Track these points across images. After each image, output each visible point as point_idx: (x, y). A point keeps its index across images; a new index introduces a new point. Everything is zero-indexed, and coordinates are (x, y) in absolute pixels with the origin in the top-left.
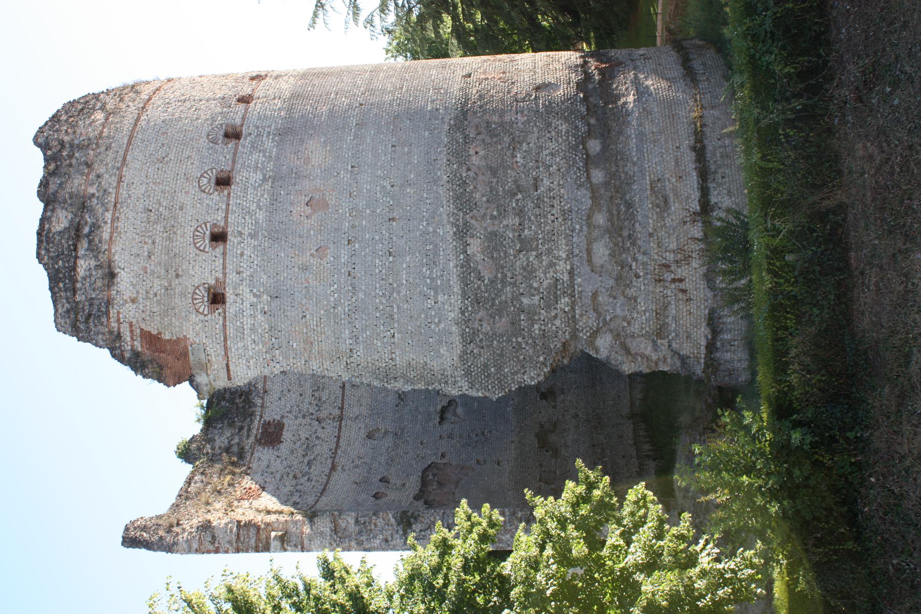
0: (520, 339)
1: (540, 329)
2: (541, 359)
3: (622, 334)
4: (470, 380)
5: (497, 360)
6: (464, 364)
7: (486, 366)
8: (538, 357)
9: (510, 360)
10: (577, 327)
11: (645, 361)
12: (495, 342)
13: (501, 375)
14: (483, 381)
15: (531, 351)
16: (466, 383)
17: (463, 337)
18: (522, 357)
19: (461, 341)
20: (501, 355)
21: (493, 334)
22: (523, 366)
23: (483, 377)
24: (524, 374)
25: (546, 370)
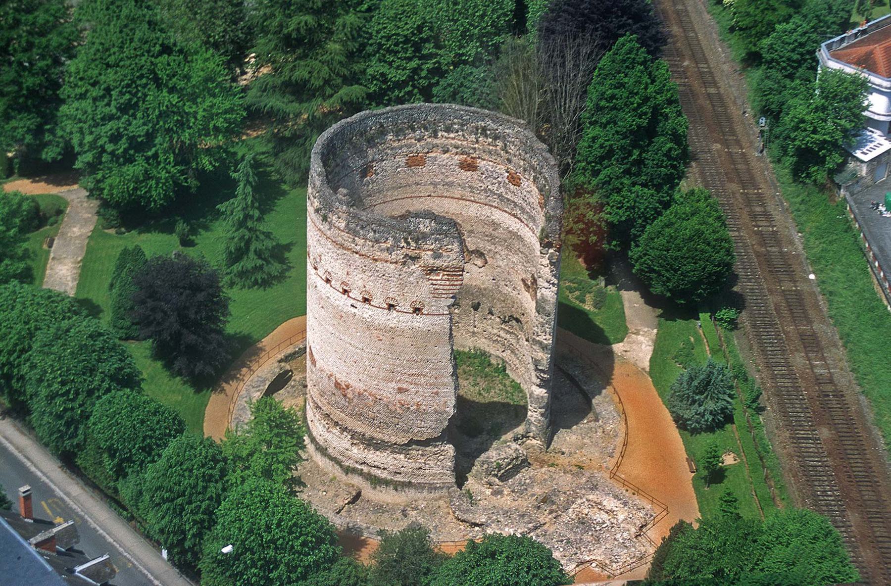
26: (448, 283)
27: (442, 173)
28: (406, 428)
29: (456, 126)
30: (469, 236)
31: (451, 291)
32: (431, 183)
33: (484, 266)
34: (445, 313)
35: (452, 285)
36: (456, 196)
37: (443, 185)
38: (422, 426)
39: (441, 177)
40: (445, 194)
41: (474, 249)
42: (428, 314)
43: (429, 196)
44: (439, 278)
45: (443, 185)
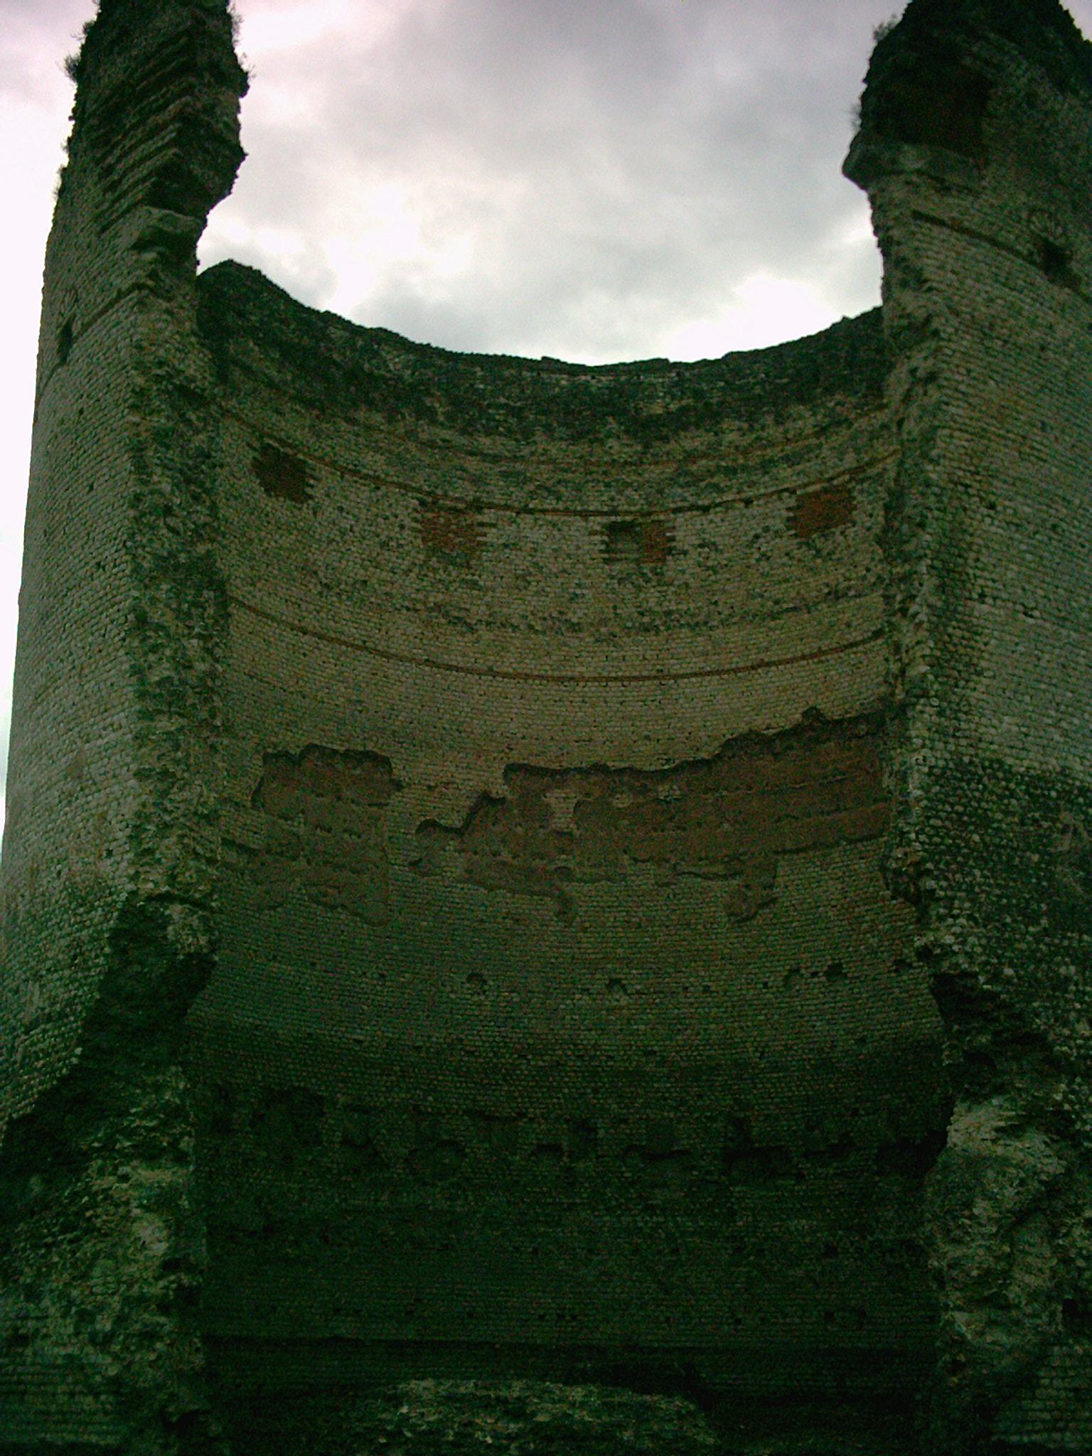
0: (1044, 922)
1: (1068, 979)
2: (1009, 971)
3: (1059, 1205)
4: (949, 773)
5: (999, 855)
6: (984, 768)
7: (984, 822)
8: (1011, 965)
9: (998, 885)
10: (1078, 1080)
11: (1002, 1265)
12: (1036, 858)
13: (966, 857)
14: (948, 808)
15: (1023, 946)
16: (941, 763)
17: (1039, 778)
18: (1008, 920)
19: (1032, 772)
20: (1009, 867)
21: (1050, 854)
22: (988, 919)
23: (960, 809)
24: (970, 917)
25: (982, 979)
35: (151, 135)
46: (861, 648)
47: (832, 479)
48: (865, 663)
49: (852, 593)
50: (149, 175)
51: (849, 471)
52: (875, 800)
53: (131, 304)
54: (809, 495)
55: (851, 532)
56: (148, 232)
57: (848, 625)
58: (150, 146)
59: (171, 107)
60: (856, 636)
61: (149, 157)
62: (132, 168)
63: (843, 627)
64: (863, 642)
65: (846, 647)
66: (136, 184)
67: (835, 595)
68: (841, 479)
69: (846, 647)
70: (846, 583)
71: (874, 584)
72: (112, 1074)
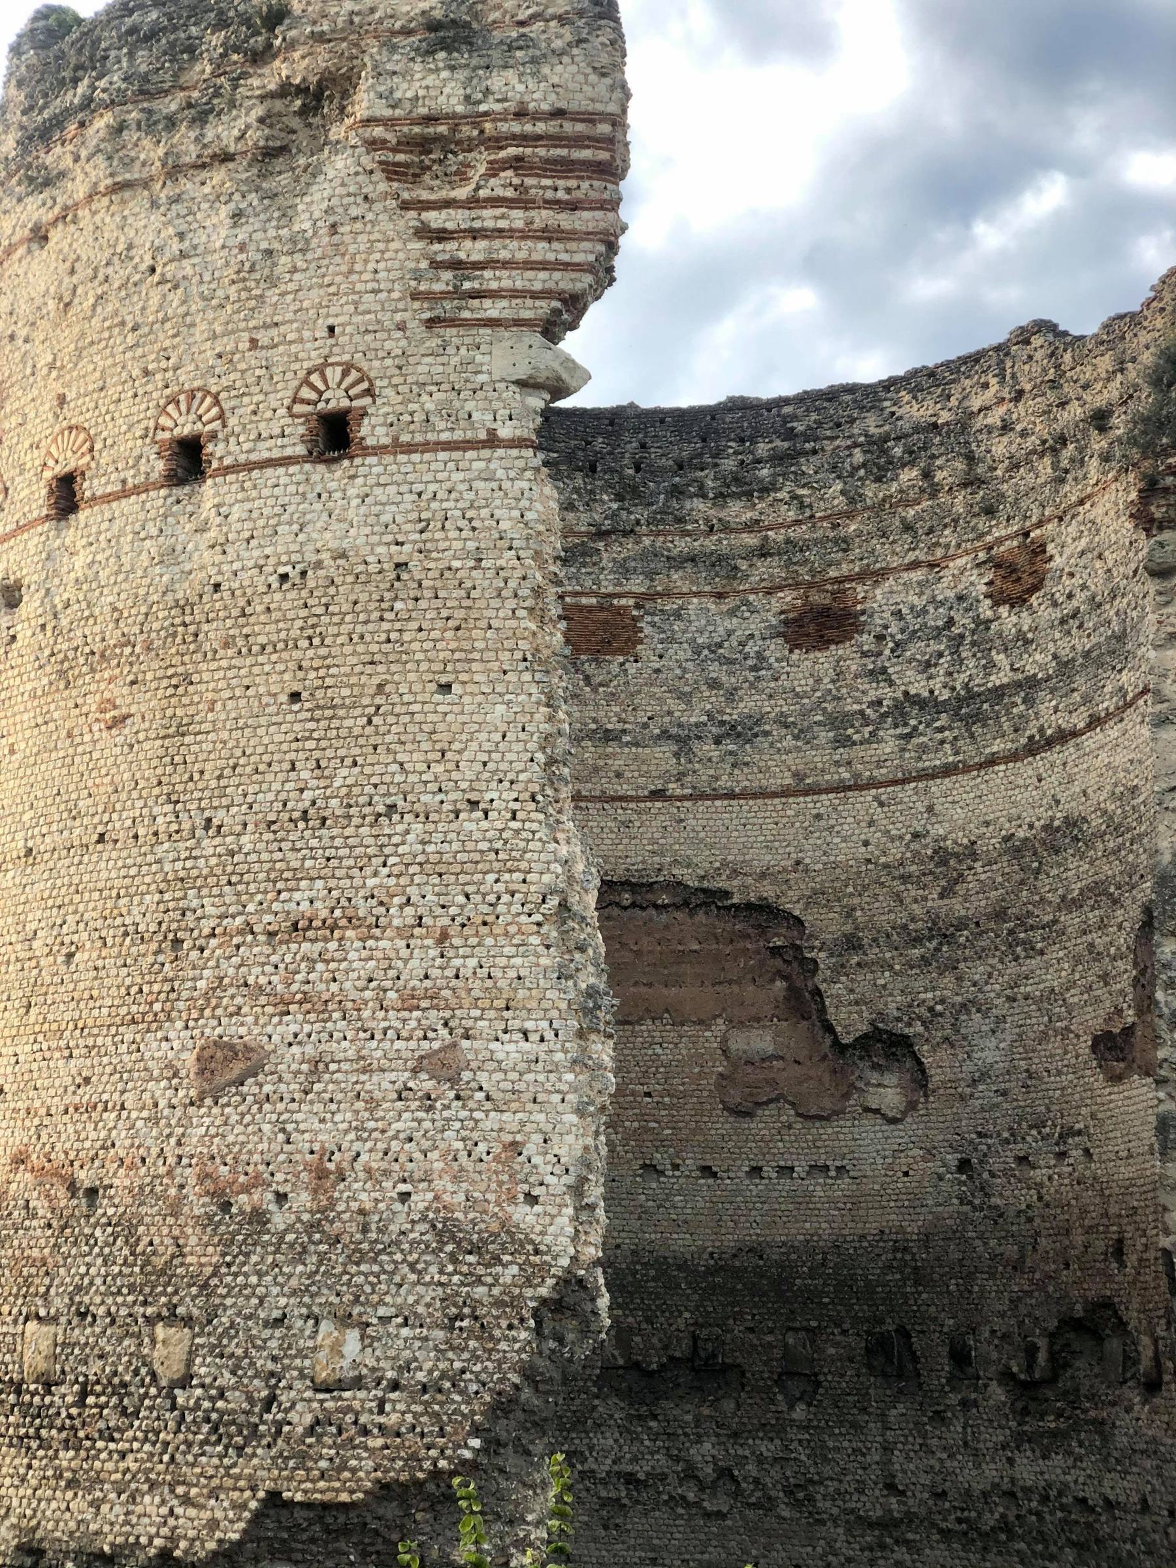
26: (517, 219)
27: (714, 684)
28: (236, 1401)
29: (765, 472)
30: (840, 969)
31: (540, 280)
32: (665, 735)
33: (912, 1106)
34: (505, 432)
35: (549, 235)
36: (774, 783)
37: (717, 741)
38: (344, 1367)
39: (709, 701)
40: (724, 782)
41: (865, 1028)
42: (398, 447)
43: (658, 795)
44: (462, 193)
45: (717, 741)
46: (632, 805)
47: (610, 595)
48: (637, 824)
49: (628, 738)
50: (545, 295)
51: (636, 596)
52: (636, 984)
53: (521, 463)
54: (581, 608)
55: (632, 668)
56: (545, 374)
57: (619, 775)
58: (541, 250)
59: (586, 215)
60: (625, 789)
61: (544, 266)
62: (506, 265)
63: (612, 775)
64: (638, 799)
65: (613, 799)
66: (515, 294)
67: (608, 736)
68: (623, 602)
69: (613, 799)
70: (619, 726)
71: (658, 737)
72: (502, 1471)
